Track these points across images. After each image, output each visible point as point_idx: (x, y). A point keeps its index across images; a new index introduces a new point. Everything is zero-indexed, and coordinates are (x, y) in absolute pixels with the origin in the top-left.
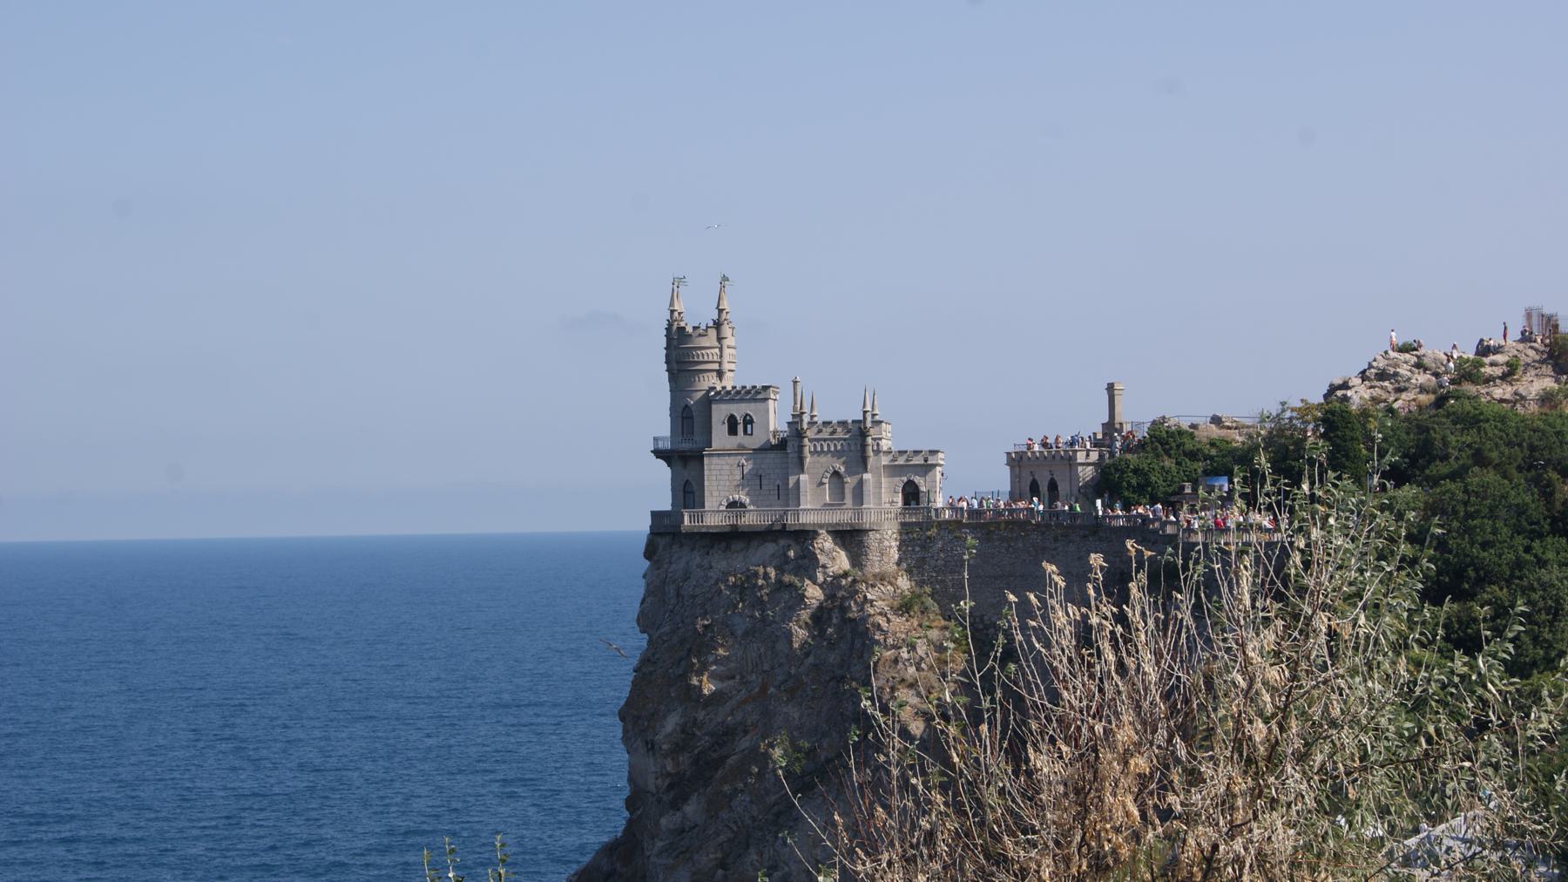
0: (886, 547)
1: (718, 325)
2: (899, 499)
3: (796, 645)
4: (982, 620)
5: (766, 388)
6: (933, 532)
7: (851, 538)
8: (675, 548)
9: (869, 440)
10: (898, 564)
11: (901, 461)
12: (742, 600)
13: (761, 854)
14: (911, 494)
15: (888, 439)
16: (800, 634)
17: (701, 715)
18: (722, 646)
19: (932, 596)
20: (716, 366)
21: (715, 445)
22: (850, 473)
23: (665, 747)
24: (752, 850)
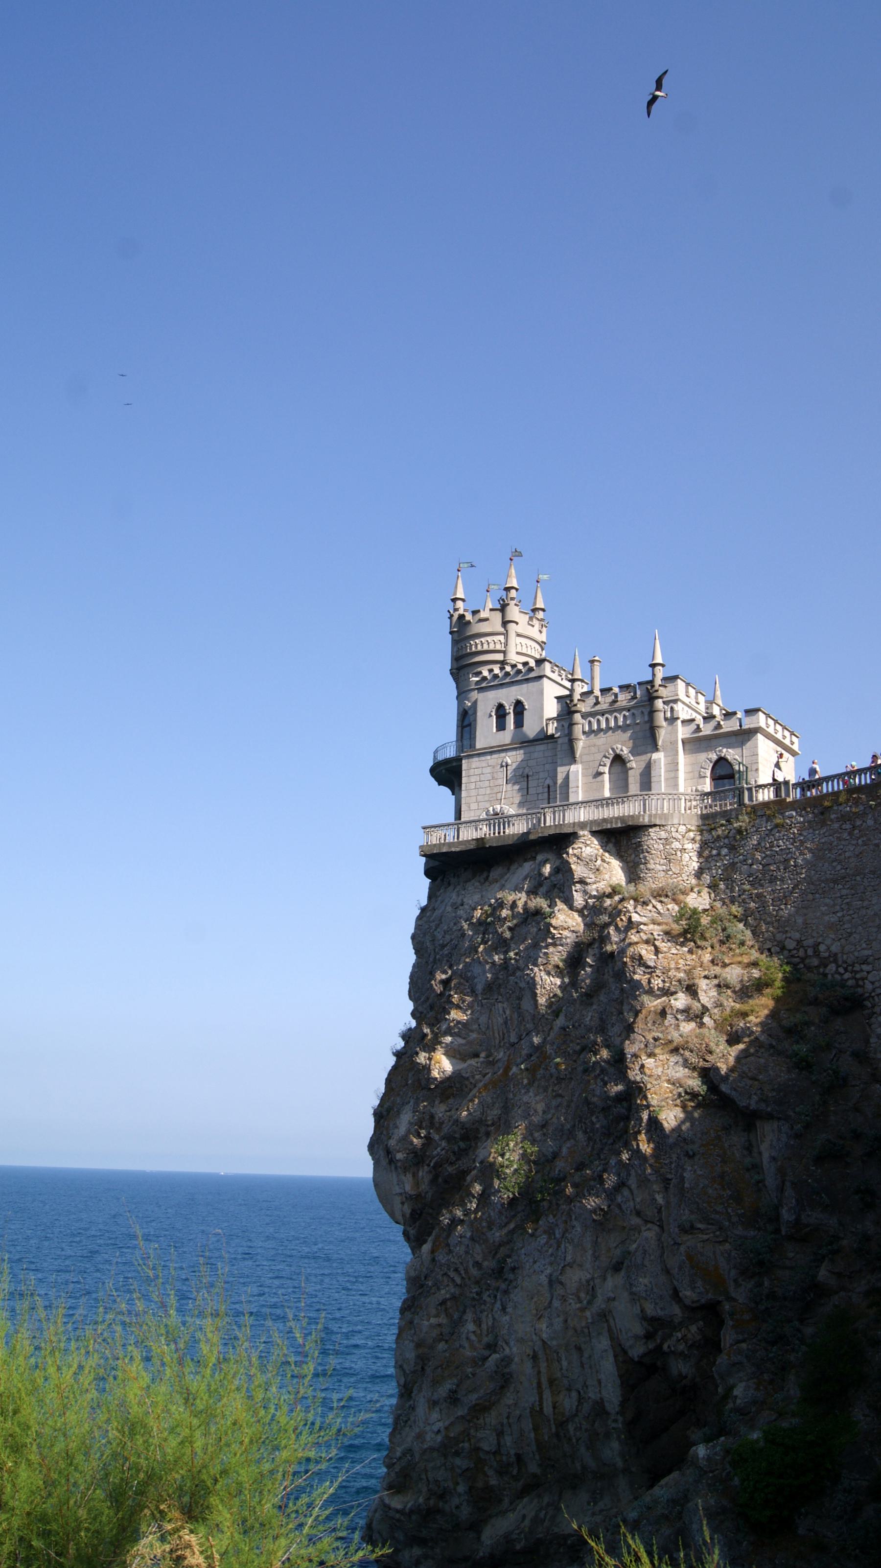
0: (678, 851)
1: (503, 608)
2: (707, 786)
3: (542, 1000)
4: (817, 953)
5: (540, 662)
6: (743, 821)
7: (623, 839)
8: (442, 891)
9: (659, 704)
10: (699, 874)
11: (707, 729)
12: (484, 942)
13: (478, 1322)
14: (725, 774)
15: (688, 704)
16: (548, 983)
17: (440, 1110)
18: (458, 1007)
19: (743, 919)
20: (499, 657)
21: (480, 744)
22: (634, 752)
23: (399, 1156)
24: (469, 1316)
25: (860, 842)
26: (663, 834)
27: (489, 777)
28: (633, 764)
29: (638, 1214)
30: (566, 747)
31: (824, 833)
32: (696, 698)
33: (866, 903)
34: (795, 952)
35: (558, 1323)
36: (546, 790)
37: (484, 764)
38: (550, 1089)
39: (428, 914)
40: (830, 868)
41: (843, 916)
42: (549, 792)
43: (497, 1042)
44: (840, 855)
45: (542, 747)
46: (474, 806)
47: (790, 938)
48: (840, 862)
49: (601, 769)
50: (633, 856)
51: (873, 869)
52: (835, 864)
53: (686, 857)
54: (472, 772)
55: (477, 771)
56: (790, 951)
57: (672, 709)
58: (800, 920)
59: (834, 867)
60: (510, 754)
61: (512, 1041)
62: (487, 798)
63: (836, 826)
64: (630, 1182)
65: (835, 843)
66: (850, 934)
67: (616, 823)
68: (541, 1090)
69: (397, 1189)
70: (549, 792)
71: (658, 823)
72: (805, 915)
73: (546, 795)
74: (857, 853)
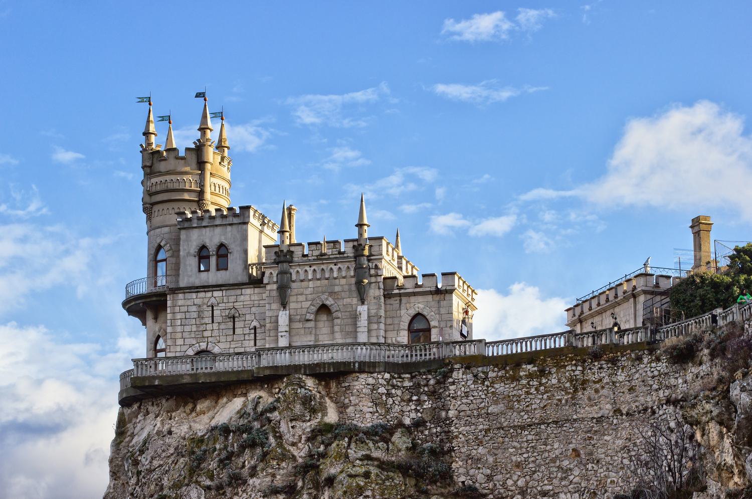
8: (140, 417)
25: (545, 396)
26: (371, 381)
27: (195, 315)
28: (340, 315)
30: (275, 293)
31: (514, 388)
32: (393, 256)
34: (486, 485)
36: (253, 331)
37: (189, 303)
39: (127, 439)
40: (518, 417)
41: (529, 457)
42: (255, 333)
44: (527, 406)
45: (248, 291)
46: (180, 342)
47: (482, 473)
48: (527, 412)
50: (343, 398)
51: (556, 420)
52: (523, 414)
53: (390, 401)
54: (177, 309)
55: (184, 309)
56: (481, 484)
57: (376, 265)
58: (491, 459)
59: (522, 416)
60: (216, 294)
62: (193, 336)
63: (524, 382)
65: (523, 397)
66: (534, 472)
67: (329, 369)
70: (255, 333)
71: (366, 370)
72: (496, 455)
73: (252, 336)
74: (542, 405)
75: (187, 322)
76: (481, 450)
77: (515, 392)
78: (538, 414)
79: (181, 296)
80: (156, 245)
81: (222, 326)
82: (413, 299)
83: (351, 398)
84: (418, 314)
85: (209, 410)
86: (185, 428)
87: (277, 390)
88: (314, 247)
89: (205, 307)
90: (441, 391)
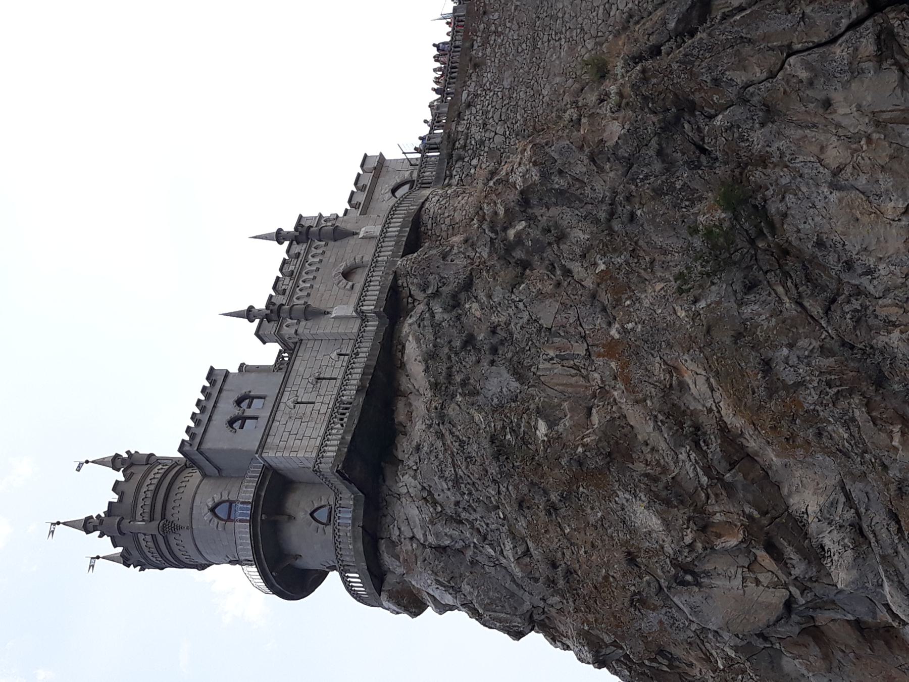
13: (890, 325)
17: (640, 467)
24: (881, 340)
29: (772, 76)
30: (309, 324)
33: (560, 15)
35: (886, 182)
37: (282, 429)
38: (642, 271)
43: (582, 381)
48: (520, 44)
49: (348, 287)
59: (523, 50)
60: (284, 399)
61: (583, 353)
63: (489, 50)
64: (739, 81)
66: (582, 29)
67: (405, 231)
68: (642, 286)
69: (737, 582)
75: (301, 432)
76: (545, 92)
77: (497, 61)
78: (524, 31)
79: (268, 440)
80: (209, 513)
81: (322, 392)
82: (376, 195)
83: (446, 215)
84: (394, 191)
85: (410, 405)
86: (418, 430)
87: (410, 300)
88: (280, 283)
89: (293, 411)
90: (473, 142)
